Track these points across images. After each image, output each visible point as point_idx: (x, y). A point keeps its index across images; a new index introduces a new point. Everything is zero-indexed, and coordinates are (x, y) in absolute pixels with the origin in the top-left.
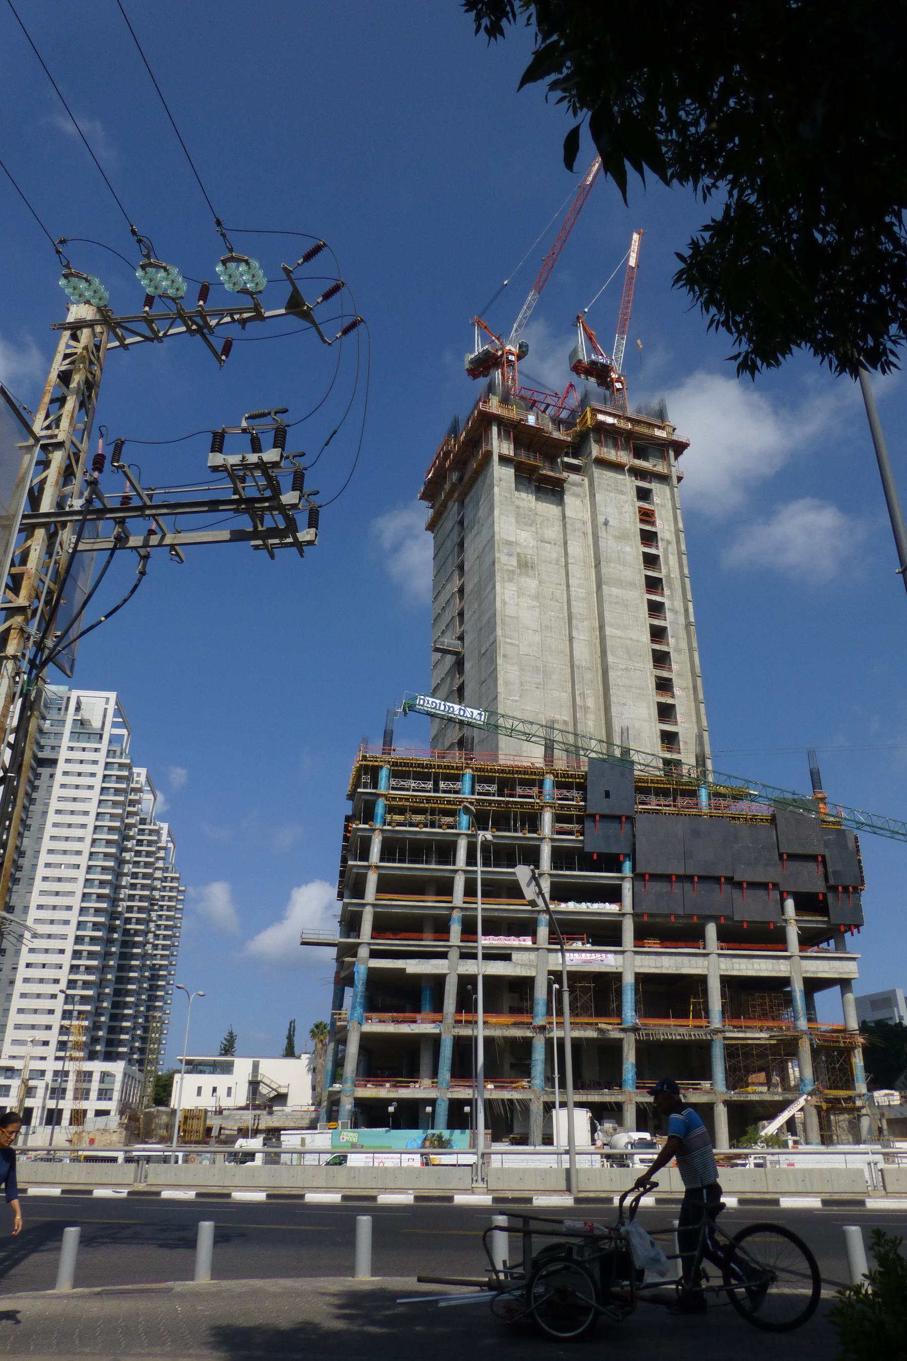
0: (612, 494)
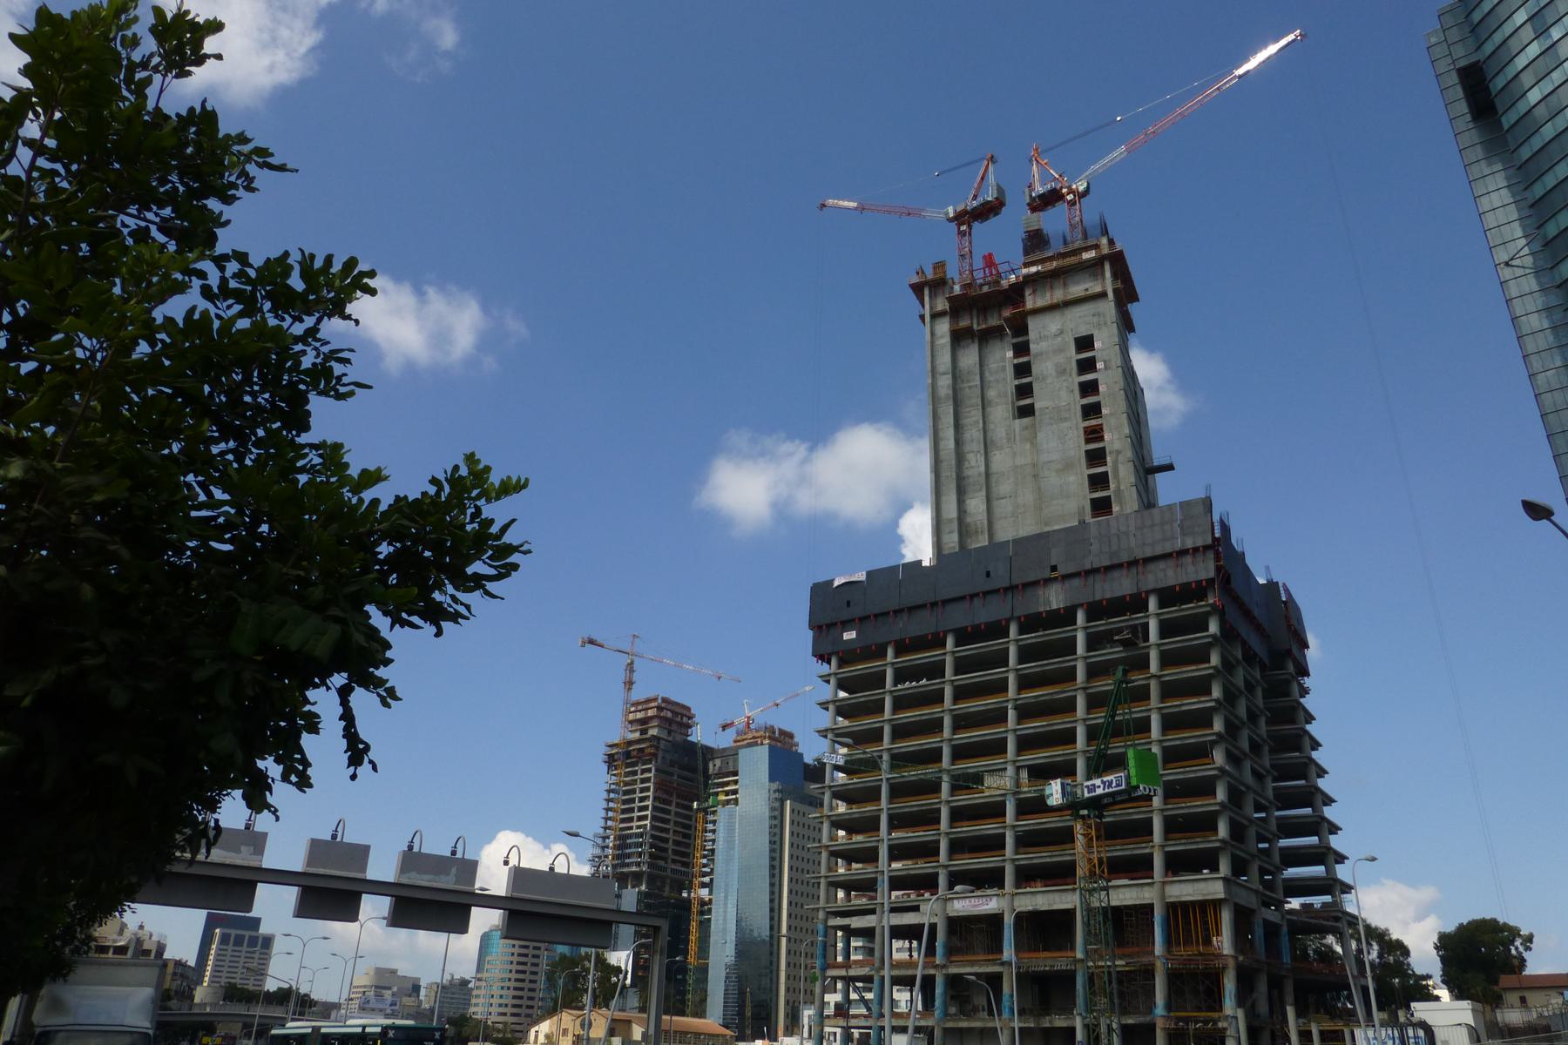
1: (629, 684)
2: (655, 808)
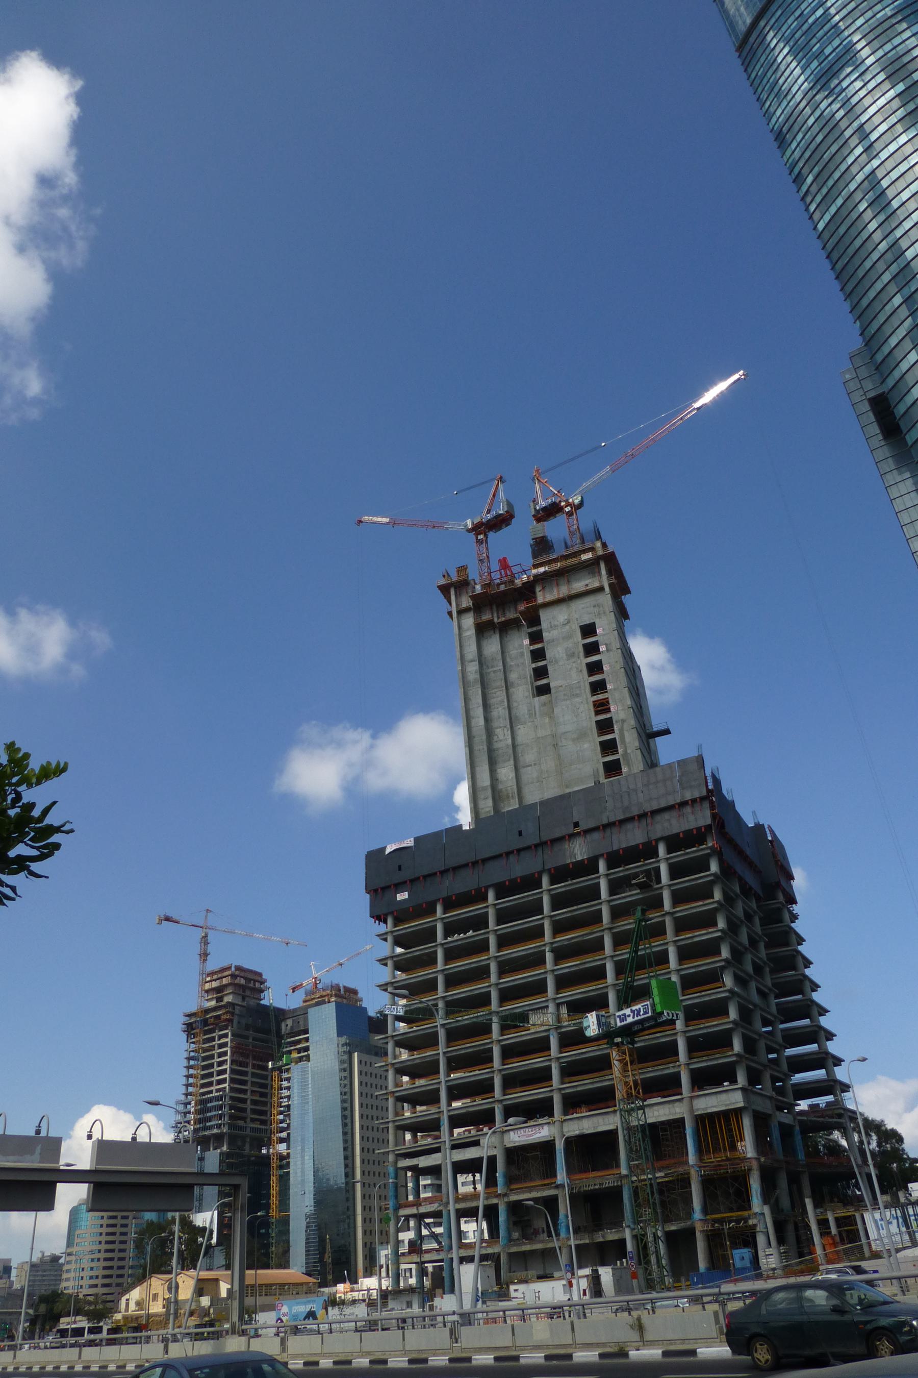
0: (568, 702)
1: (204, 956)
2: (233, 1071)
